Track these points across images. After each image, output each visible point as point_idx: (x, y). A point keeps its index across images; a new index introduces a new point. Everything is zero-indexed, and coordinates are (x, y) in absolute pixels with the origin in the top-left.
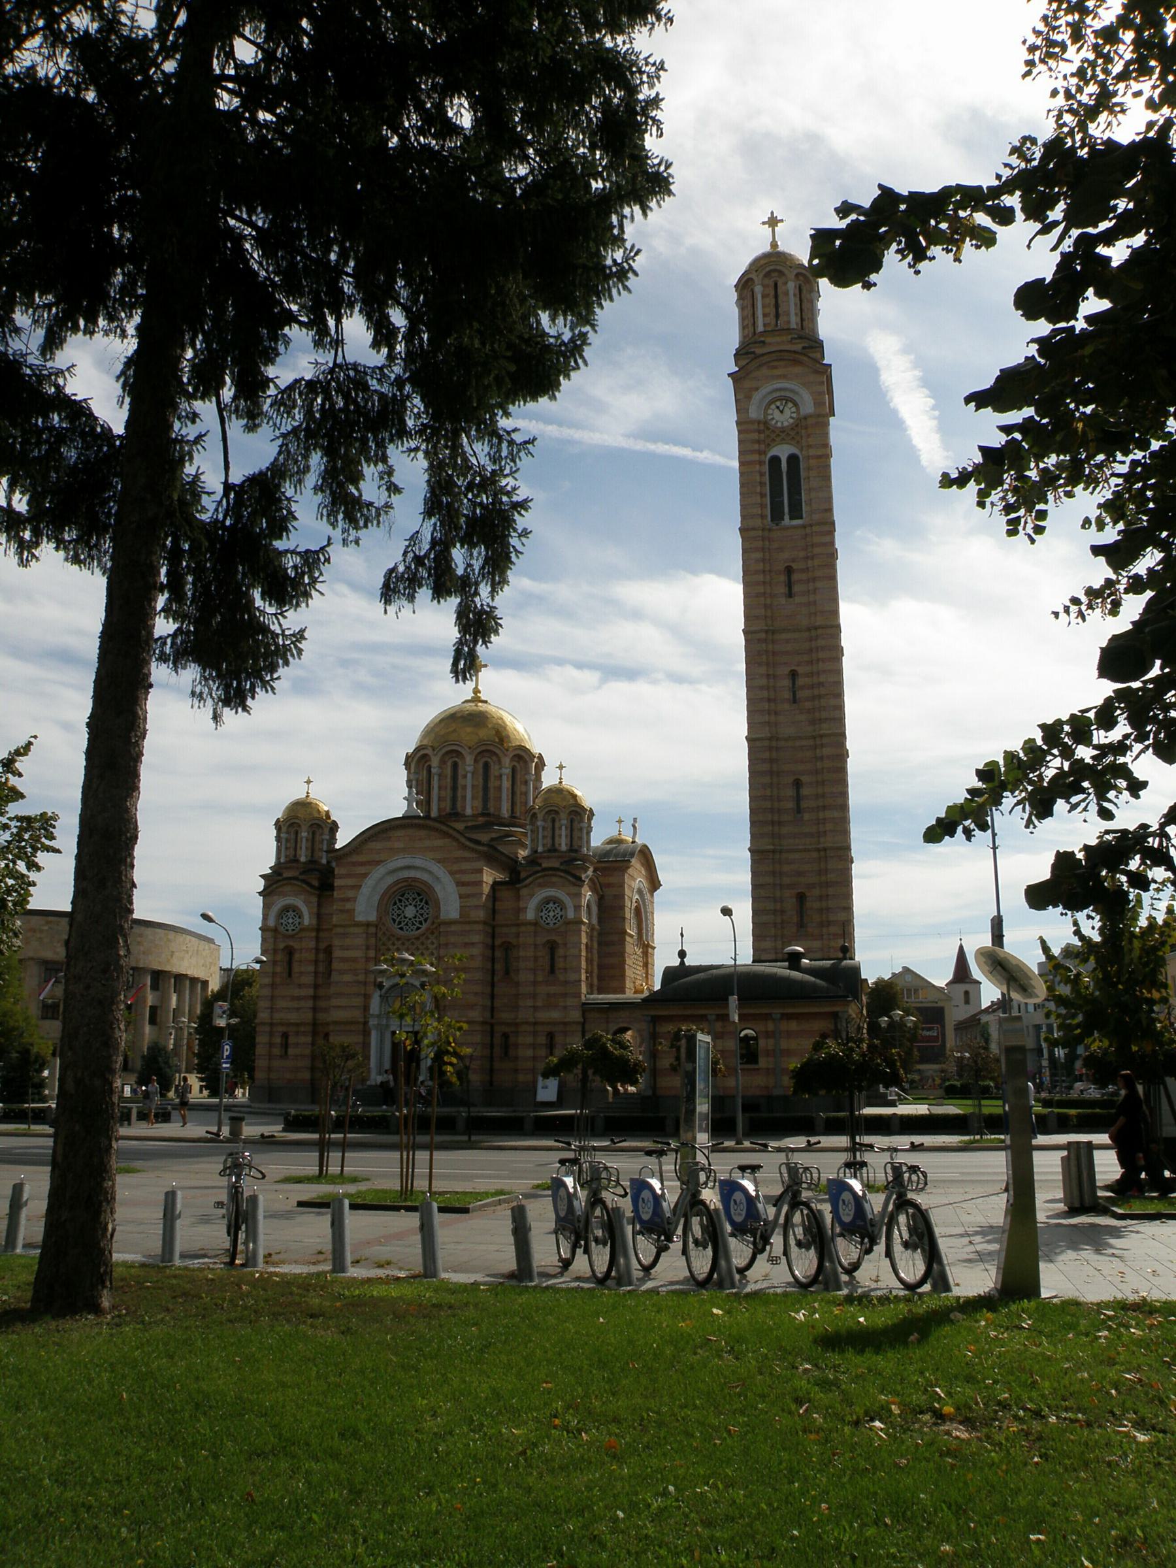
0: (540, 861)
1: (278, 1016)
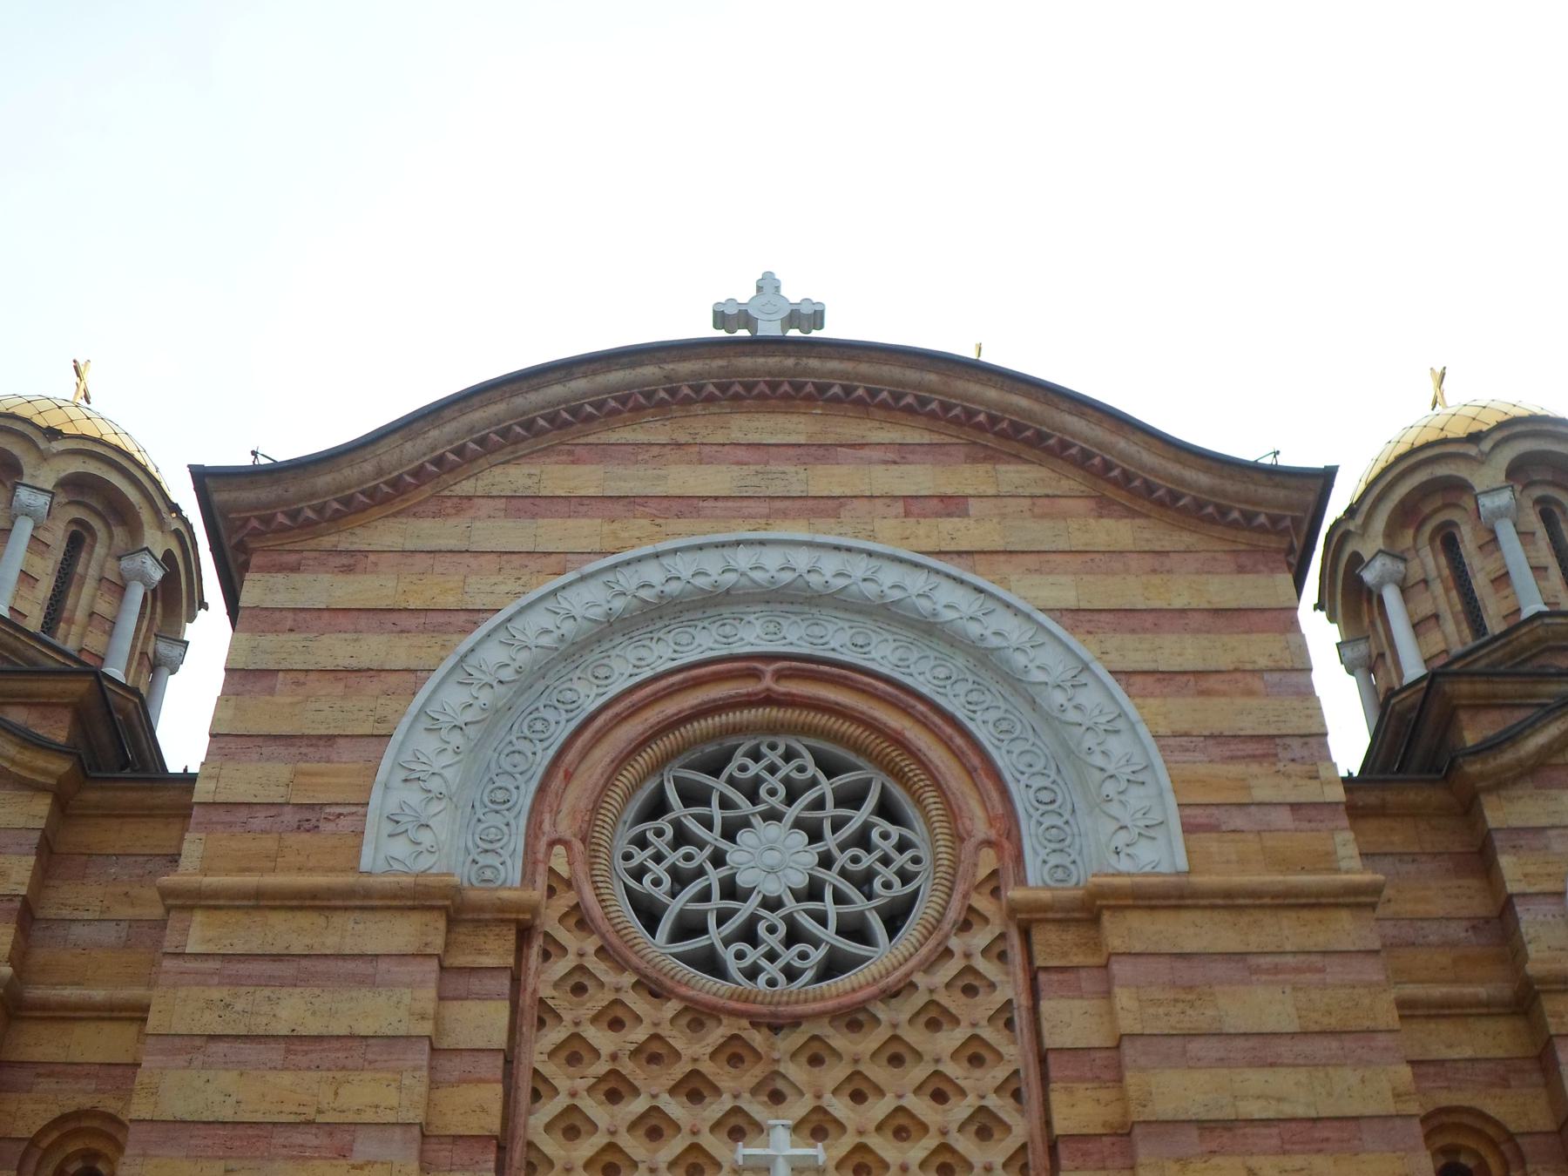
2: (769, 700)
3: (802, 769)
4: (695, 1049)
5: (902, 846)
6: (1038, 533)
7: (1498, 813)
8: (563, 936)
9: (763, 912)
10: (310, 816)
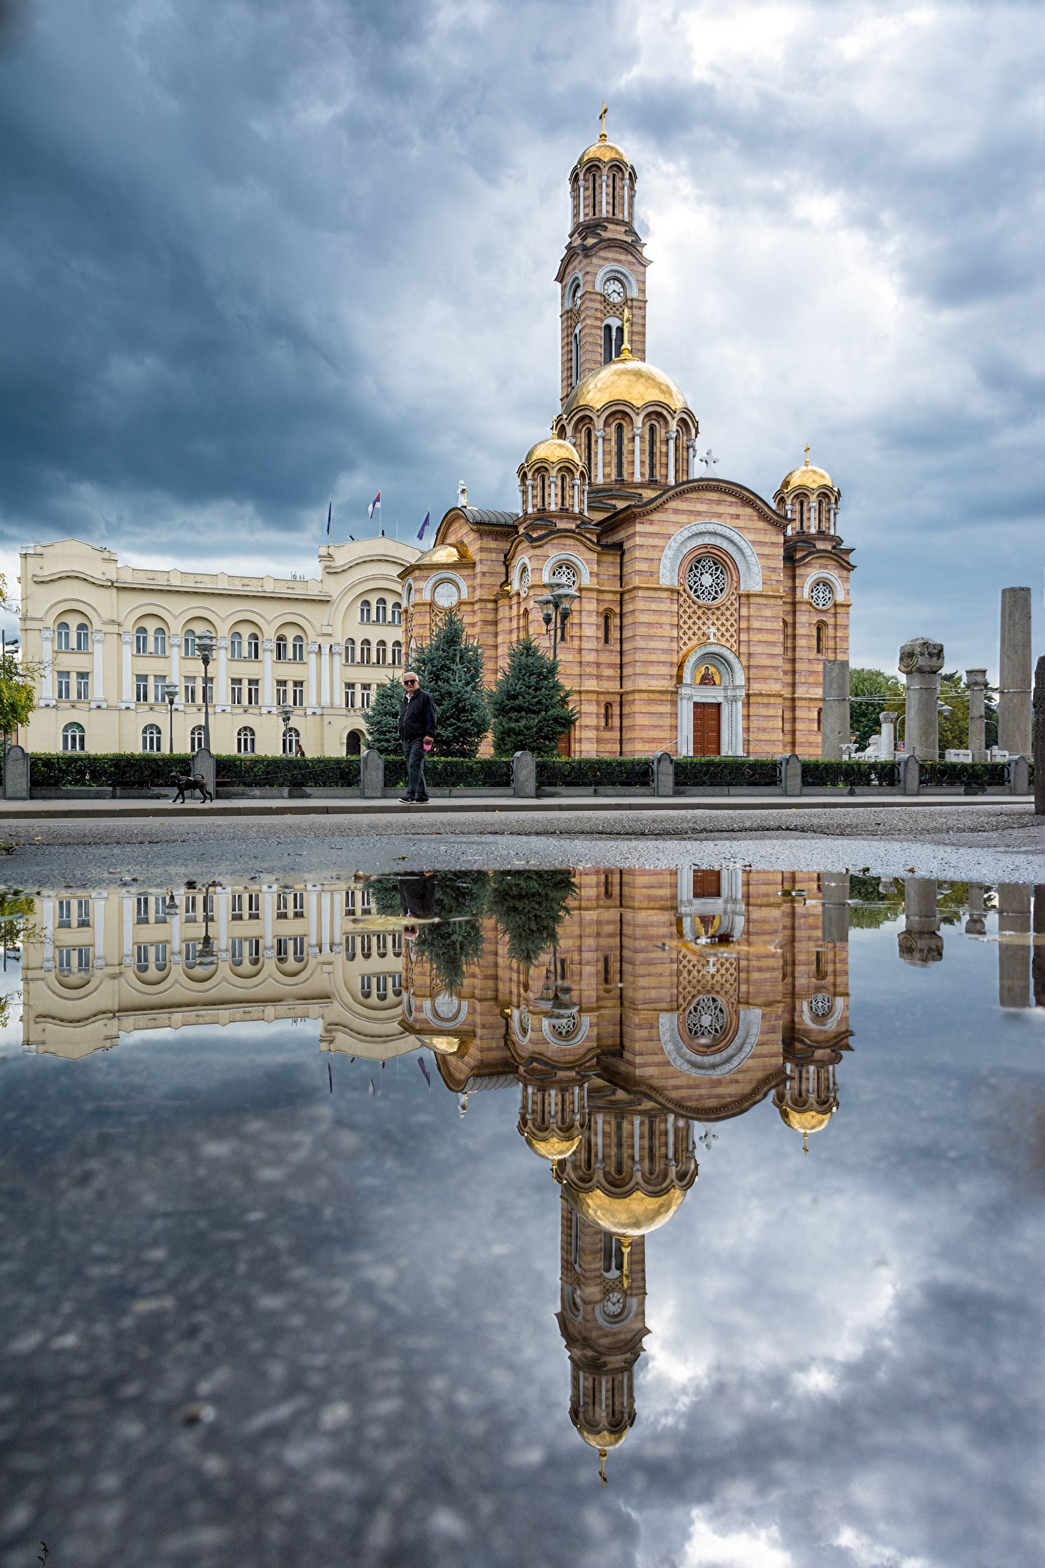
0: (814, 542)
2: (709, 552)
4: (700, 612)
6: (750, 524)
7: (799, 571)
8: (683, 593)
10: (652, 574)
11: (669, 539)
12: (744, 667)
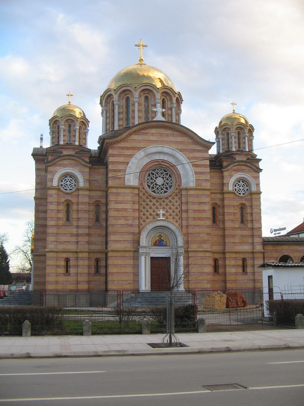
0: (235, 156)
1: (61, 247)
3: (162, 171)
5: (171, 180)
8: (142, 190)
9: (159, 187)
11: (132, 157)
12: (184, 235)
